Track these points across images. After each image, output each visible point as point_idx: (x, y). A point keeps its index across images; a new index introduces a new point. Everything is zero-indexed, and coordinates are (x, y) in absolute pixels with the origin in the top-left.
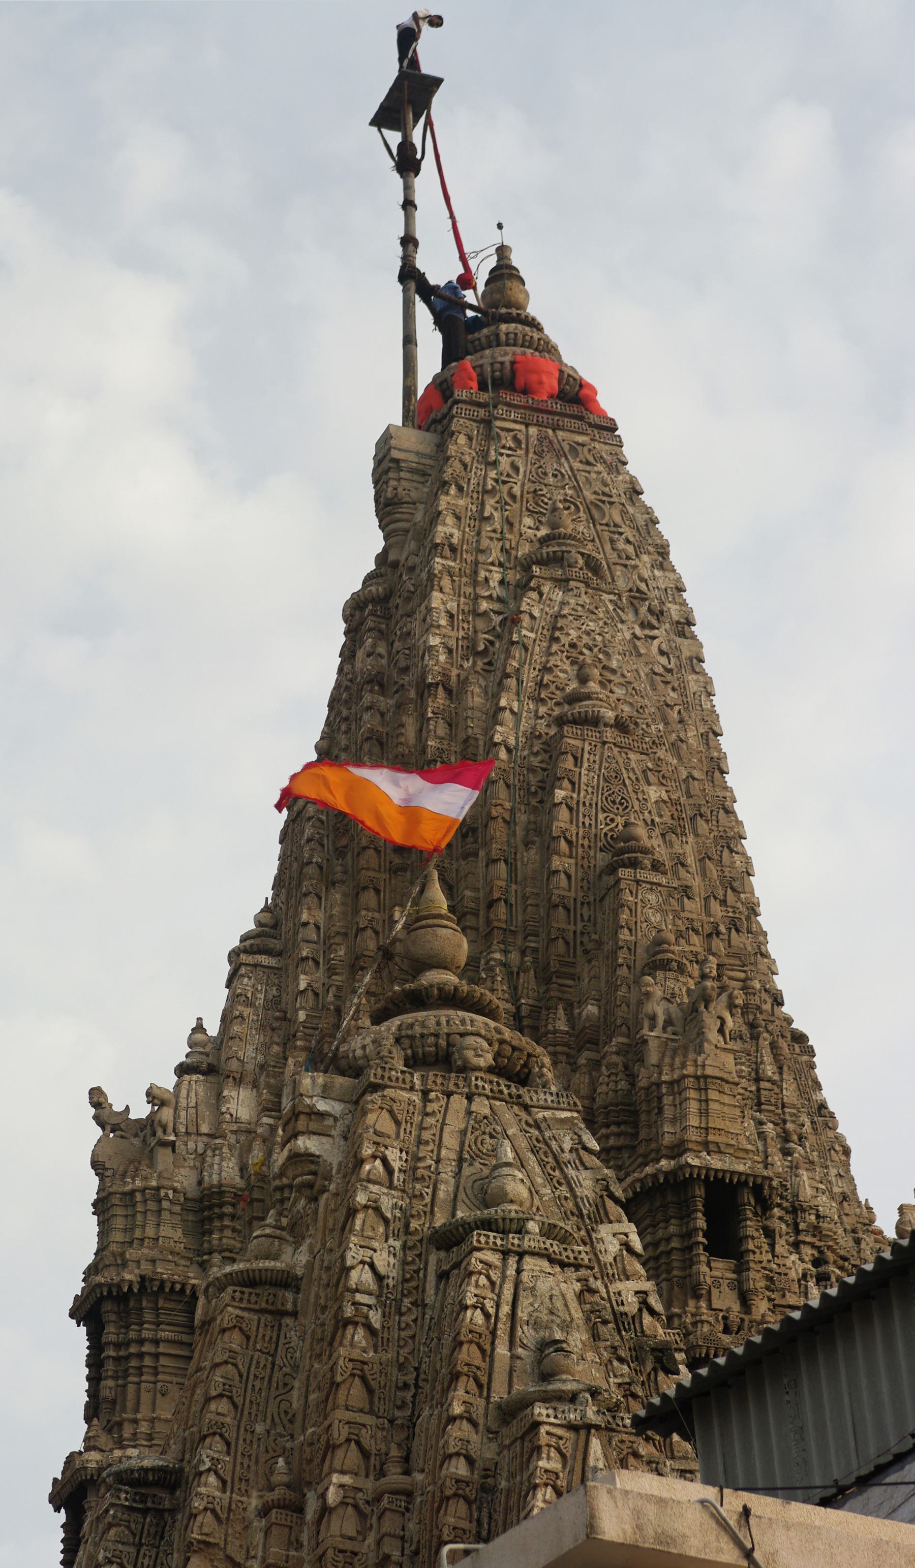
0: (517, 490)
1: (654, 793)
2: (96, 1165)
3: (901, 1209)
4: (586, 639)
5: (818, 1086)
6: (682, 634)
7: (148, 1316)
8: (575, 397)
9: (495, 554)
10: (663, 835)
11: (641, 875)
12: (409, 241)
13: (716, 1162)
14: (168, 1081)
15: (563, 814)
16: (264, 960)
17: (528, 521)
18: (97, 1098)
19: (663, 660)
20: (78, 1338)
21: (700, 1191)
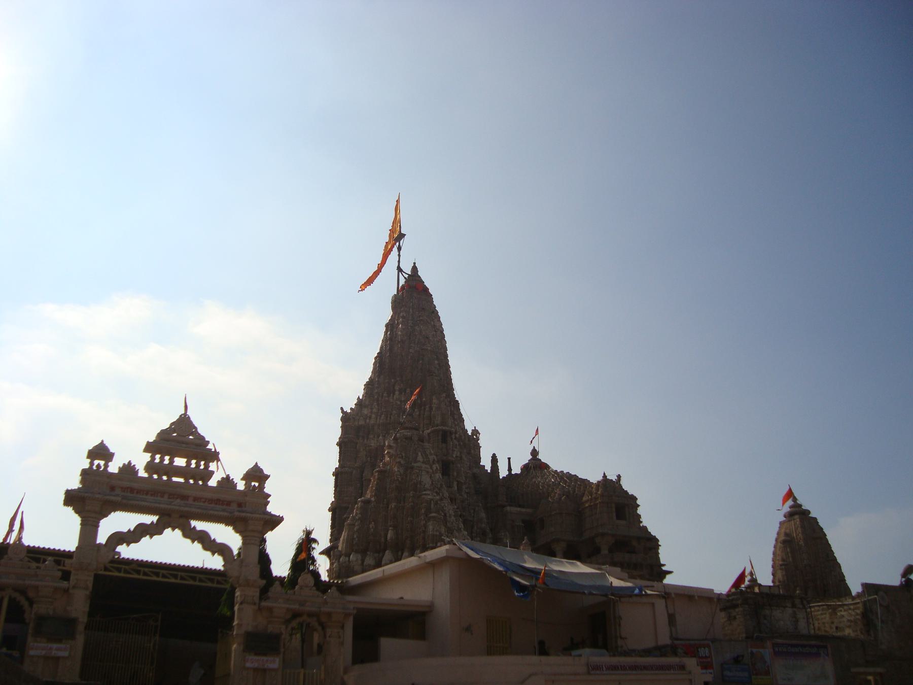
1: (436, 362)
12: (399, 262)
18: (342, 408)
20: (337, 449)
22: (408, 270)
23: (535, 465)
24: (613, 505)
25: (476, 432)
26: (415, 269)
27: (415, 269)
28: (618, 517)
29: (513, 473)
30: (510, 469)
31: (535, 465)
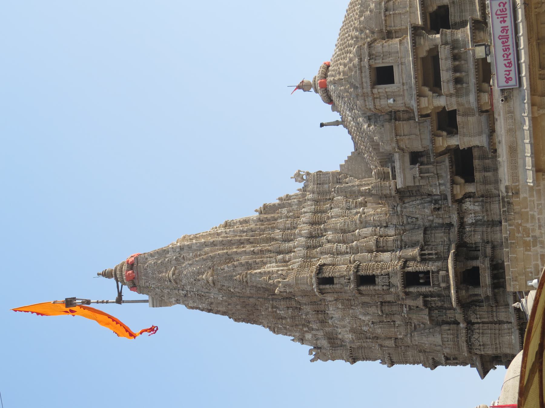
0: (160, 284)
2: (326, 360)
3: (296, 181)
4: (193, 277)
5: (274, 205)
6: (183, 249)
7: (357, 355)
8: (131, 266)
9: (176, 292)
10: (235, 267)
11: (249, 281)
14: (307, 348)
15: (237, 290)
16: (276, 330)
17: (166, 283)
18: (312, 361)
19: (191, 254)
21: (322, 287)
23: (324, 87)
24: (375, 91)
25: (298, 177)
26: (107, 274)
27: (107, 274)
28: (391, 81)
29: (340, 120)
30: (337, 123)
31: (324, 87)
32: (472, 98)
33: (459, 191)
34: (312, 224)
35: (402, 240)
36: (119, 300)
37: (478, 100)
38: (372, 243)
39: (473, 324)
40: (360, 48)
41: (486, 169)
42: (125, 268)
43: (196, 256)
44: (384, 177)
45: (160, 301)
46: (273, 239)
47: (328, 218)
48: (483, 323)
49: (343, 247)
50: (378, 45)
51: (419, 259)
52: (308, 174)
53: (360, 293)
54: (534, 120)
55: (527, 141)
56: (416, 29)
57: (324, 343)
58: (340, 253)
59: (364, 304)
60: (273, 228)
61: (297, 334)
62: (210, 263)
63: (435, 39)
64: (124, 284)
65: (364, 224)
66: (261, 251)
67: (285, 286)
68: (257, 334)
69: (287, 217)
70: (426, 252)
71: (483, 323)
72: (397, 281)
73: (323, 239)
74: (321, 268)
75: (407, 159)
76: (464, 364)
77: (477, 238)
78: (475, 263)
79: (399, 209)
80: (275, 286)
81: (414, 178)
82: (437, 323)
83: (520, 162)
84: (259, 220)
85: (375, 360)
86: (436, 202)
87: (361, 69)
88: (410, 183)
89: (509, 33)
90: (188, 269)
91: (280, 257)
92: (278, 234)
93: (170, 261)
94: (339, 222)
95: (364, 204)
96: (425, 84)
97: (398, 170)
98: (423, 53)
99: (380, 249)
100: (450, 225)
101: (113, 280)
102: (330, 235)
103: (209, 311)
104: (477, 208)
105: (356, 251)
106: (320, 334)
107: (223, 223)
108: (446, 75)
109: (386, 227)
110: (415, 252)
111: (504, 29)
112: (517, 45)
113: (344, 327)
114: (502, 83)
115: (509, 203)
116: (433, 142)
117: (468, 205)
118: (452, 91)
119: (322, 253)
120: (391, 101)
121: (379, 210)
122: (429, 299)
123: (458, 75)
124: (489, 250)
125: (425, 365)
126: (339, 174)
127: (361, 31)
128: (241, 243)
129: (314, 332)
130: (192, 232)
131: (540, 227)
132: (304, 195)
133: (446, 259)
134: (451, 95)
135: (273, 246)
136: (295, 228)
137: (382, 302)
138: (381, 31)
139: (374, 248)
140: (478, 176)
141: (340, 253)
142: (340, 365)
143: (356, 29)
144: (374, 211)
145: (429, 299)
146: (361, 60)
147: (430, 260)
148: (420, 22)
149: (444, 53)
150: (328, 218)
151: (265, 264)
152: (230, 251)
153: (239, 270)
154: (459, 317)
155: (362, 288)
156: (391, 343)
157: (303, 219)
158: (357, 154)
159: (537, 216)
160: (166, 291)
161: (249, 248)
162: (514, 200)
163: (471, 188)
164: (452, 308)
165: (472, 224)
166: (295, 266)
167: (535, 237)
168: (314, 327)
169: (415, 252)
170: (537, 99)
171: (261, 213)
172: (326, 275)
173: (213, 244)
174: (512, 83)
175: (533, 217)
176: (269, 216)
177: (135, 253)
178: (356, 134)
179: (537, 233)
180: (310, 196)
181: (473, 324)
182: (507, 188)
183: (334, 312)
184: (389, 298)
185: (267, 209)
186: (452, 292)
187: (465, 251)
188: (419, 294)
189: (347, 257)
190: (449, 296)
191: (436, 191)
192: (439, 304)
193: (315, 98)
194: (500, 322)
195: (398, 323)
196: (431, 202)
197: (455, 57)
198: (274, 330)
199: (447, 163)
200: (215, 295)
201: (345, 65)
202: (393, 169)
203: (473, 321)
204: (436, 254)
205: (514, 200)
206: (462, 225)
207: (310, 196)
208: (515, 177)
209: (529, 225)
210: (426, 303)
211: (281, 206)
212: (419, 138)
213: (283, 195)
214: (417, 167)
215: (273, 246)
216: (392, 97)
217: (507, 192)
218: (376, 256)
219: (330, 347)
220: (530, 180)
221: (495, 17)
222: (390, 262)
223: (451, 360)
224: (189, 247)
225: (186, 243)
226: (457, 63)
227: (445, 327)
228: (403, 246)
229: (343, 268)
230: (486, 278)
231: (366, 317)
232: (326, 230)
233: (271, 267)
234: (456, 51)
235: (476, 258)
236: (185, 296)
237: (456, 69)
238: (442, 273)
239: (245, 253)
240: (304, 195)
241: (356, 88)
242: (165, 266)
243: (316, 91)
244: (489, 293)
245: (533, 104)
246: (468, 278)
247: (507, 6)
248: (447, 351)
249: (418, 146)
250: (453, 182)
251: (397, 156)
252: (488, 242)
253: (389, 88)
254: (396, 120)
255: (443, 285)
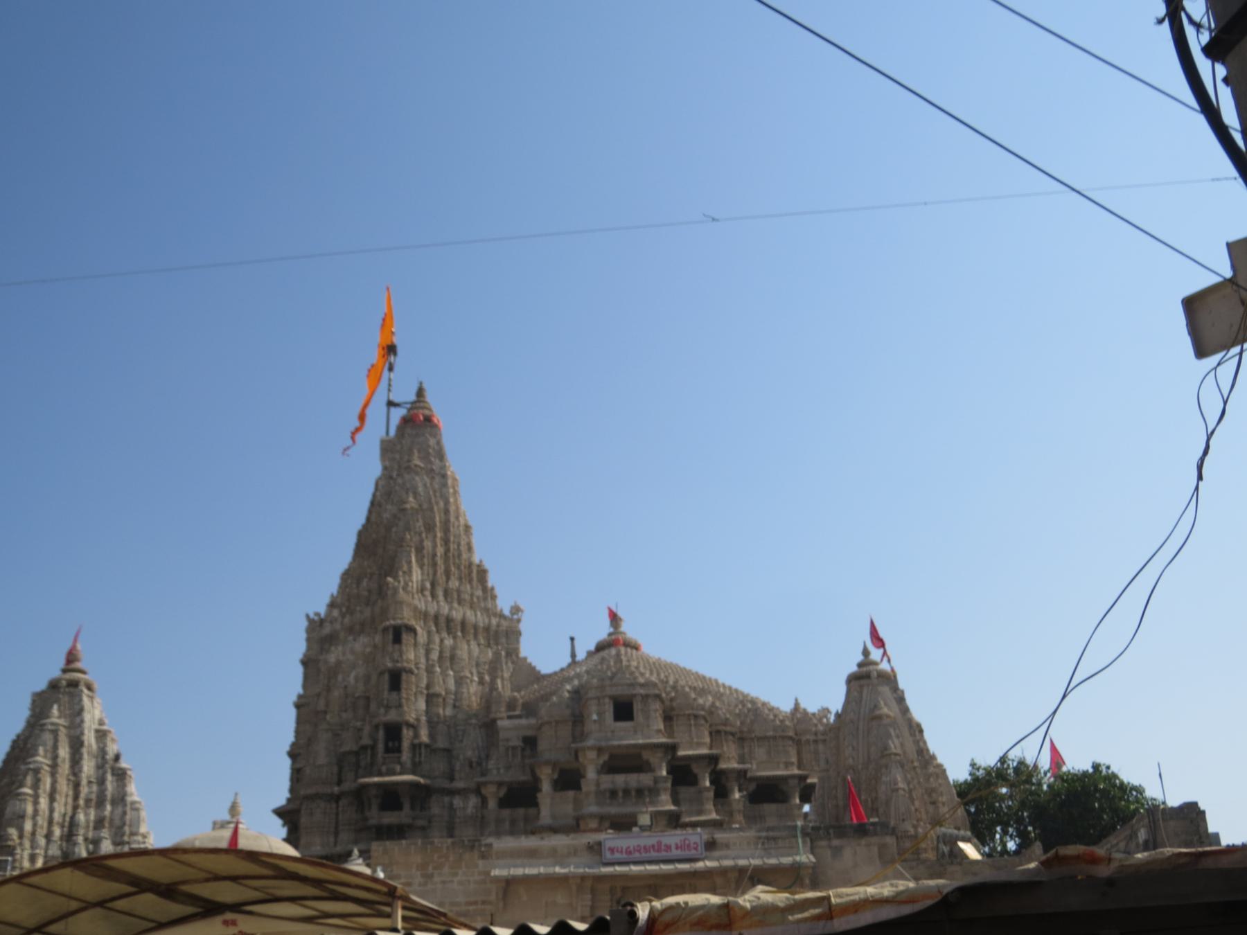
8: (428, 419)
13: (392, 622)
18: (308, 616)
21: (391, 631)
22: (406, 394)
23: (615, 644)
24: (607, 700)
25: (516, 609)
26: (420, 393)
27: (420, 393)
30: (573, 655)
31: (615, 644)
32: (594, 809)
33: (489, 791)
34: (463, 623)
35: (438, 723)
36: (390, 404)
37: (592, 816)
38: (439, 689)
39: (337, 802)
40: (655, 685)
41: (513, 822)
42: (427, 412)
43: (435, 492)
44: (511, 705)
45: (388, 448)
46: (448, 579)
47: (468, 642)
48: (337, 814)
49: (435, 656)
50: (656, 706)
51: (416, 741)
52: (519, 621)
53: (382, 673)
54: (564, 879)
55: (542, 870)
56: (672, 748)
57: (327, 630)
58: (428, 652)
59: (367, 678)
60: (460, 579)
61: (339, 600)
62: (425, 506)
63: (660, 768)
64: (409, 410)
65: (460, 681)
66: (435, 565)
67: (395, 590)
68: (343, 556)
69: (472, 595)
70: (423, 750)
71: (337, 814)
72: (392, 716)
73: (444, 634)
74: (412, 630)
75: (529, 733)
76: (292, 790)
77: (435, 809)
78: (407, 806)
79: (474, 721)
80: (396, 578)
81: (508, 740)
82: (341, 760)
83: (519, 862)
84: (470, 565)
85: (305, 686)
86: (479, 764)
87: (632, 685)
88: (502, 735)
89: (664, 854)
90: (421, 482)
91: (428, 585)
92: (454, 584)
93: (431, 462)
94: (463, 652)
95: (481, 682)
96: (612, 757)
97: (517, 722)
98: (646, 755)
99: (431, 698)
100: (452, 779)
101: (413, 398)
102: (449, 642)
103: (372, 503)
104: (469, 811)
105: (429, 670)
106: (338, 626)
107: (470, 523)
108: (620, 780)
109: (455, 706)
110: (424, 737)
111: (668, 848)
112: (651, 862)
113: (344, 654)
114: (609, 844)
115: (472, 847)
116: (547, 763)
117: (473, 801)
118: (603, 787)
119: (429, 633)
120: (595, 717)
121: (473, 698)
122: (369, 752)
123: (620, 794)
124: (421, 823)
125: (293, 745)
126: (517, 656)
127: (674, 688)
128: (446, 542)
129: (340, 619)
130: (462, 489)
131: (444, 882)
132: (495, 615)
133: (414, 773)
134: (598, 784)
135: (441, 578)
136: (459, 603)
137: (368, 699)
138: (672, 709)
139: (432, 691)
140: (506, 813)
141: (428, 652)
142: (299, 647)
143: (676, 682)
144: (473, 693)
145: (369, 752)
146: (642, 685)
147: (414, 756)
148: (681, 753)
149: (645, 779)
150: (468, 642)
151: (421, 566)
152: (438, 530)
153: (416, 539)
154: (348, 786)
155: (386, 677)
156: (321, 705)
157: (469, 613)
158: (536, 676)
159: (456, 879)
160: (397, 456)
161: (440, 550)
162: (476, 854)
163: (492, 804)
164: (357, 777)
165: (451, 804)
166: (416, 602)
167: (432, 876)
168: (347, 620)
169: (424, 737)
170: (589, 884)
171: (479, 566)
172: (404, 636)
173: (447, 512)
174: (608, 856)
175: (456, 874)
176: (474, 575)
177: (442, 425)
178: (559, 677)
179: (437, 879)
180: (494, 621)
181: (337, 802)
182: (490, 845)
183: (361, 644)
184: (373, 706)
185: (482, 573)
186: (376, 779)
187: (420, 795)
188: (375, 741)
189: (423, 660)
190: (371, 775)
191: (491, 764)
192: (363, 764)
193: (602, 631)
194: (336, 834)
195: (344, 715)
196: (479, 757)
197: (640, 792)
198: (346, 575)
199: (523, 778)
200: (389, 510)
201: (637, 668)
202: (519, 717)
203: (341, 803)
204: (420, 762)
205: (476, 854)
206: (452, 793)
207: (494, 621)
208: (503, 855)
209: (446, 870)
210: (364, 748)
211: (485, 589)
212: (552, 747)
213: (497, 591)
214: (519, 743)
215: (441, 578)
216: (599, 716)
217: (486, 845)
218: (421, 693)
219: (321, 635)
220: (496, 872)
221: (682, 838)
222: (415, 709)
223: (297, 776)
224: (445, 485)
225: (450, 482)
226: (633, 793)
227: (335, 769)
228: (432, 724)
229: (411, 655)
230: (389, 818)
231: (352, 678)
232: (455, 638)
233: (417, 574)
234: (646, 793)
235: (413, 808)
236: (391, 477)
237: (626, 792)
238: (398, 768)
239: (435, 546)
240: (495, 615)
241: (611, 678)
242: (426, 457)
243: (610, 634)
244: (373, 822)
245: (583, 878)
246: (391, 798)
247: (693, 852)
248: (308, 771)
249: (543, 745)
250: (500, 784)
251: (533, 721)
252: (430, 822)
253: (609, 715)
254: (574, 723)
255: (384, 769)
